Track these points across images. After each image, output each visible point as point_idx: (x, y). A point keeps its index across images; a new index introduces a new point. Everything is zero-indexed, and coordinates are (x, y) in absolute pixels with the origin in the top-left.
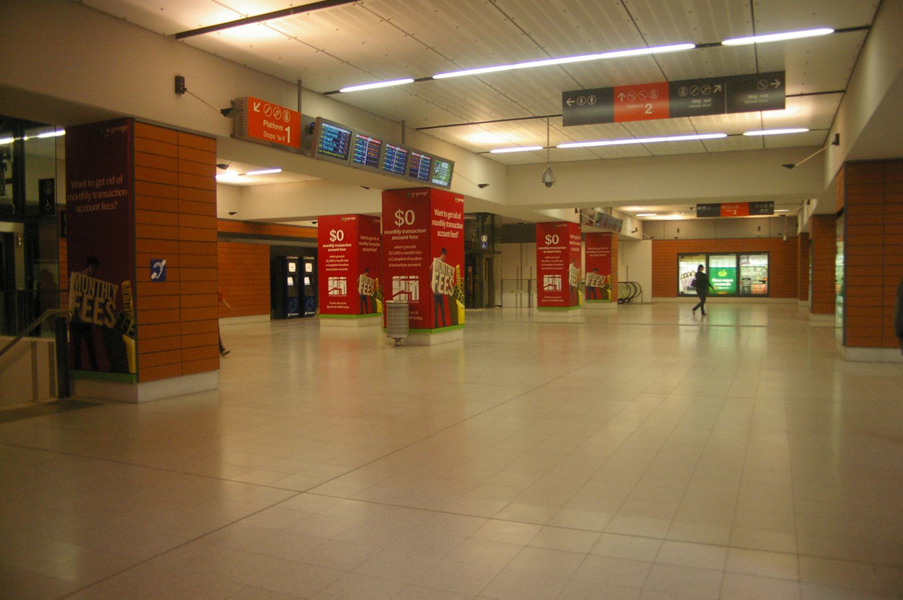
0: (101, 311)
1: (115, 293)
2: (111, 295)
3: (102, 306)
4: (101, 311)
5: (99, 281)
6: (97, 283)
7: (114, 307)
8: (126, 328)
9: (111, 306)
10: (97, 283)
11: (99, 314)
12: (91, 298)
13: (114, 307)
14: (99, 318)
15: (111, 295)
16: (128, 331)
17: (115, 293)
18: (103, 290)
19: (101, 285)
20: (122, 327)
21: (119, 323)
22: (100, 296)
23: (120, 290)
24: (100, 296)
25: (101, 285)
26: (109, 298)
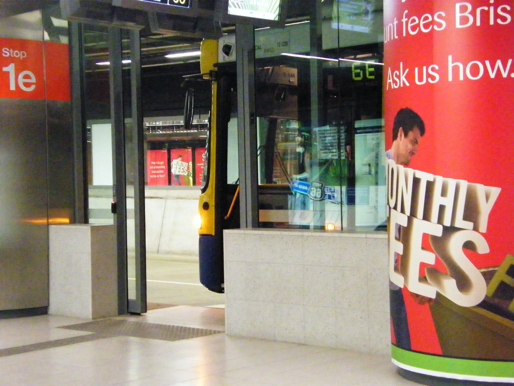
0: (430, 258)
3: (435, 244)
4: (430, 258)
5: (425, 177)
6: (416, 181)
7: (483, 247)
9: (469, 247)
10: (416, 181)
11: (423, 265)
14: (422, 279)
15: (471, 213)
18: (437, 200)
22: (426, 217)
24: (426, 217)
25: (430, 186)
26: (460, 222)
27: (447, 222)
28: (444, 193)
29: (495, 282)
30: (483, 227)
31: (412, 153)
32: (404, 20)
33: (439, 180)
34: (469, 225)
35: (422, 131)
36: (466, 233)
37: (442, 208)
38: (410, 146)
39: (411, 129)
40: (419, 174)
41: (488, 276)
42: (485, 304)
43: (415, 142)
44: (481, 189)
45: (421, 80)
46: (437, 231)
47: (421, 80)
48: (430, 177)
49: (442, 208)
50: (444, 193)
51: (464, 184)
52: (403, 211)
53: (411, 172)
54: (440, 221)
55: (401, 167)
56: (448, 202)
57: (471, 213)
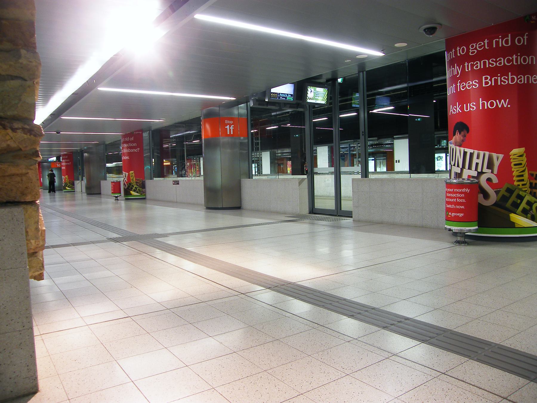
1: (497, 164)
6: (465, 153)
7: (495, 180)
8: (516, 206)
9: (489, 180)
10: (465, 153)
12: (458, 170)
13: (495, 180)
15: (490, 166)
16: (521, 208)
17: (497, 164)
19: (471, 155)
20: (508, 204)
21: (504, 199)
22: (470, 168)
24: (470, 168)
25: (471, 155)
26: (485, 170)
27: (479, 170)
28: (478, 157)
29: (500, 195)
30: (495, 172)
31: (463, 141)
32: (458, 84)
33: (476, 152)
34: (490, 171)
35: (468, 132)
36: (488, 174)
37: (477, 164)
38: (462, 138)
39: (463, 131)
40: (466, 150)
41: (497, 193)
42: (496, 204)
43: (464, 136)
44: (495, 155)
45: (467, 109)
46: (475, 174)
47: (467, 109)
48: (472, 151)
49: (477, 164)
50: (478, 157)
51: (487, 153)
52: (458, 166)
53: (462, 149)
54: (476, 169)
55: (457, 147)
56: (480, 161)
57: (490, 166)
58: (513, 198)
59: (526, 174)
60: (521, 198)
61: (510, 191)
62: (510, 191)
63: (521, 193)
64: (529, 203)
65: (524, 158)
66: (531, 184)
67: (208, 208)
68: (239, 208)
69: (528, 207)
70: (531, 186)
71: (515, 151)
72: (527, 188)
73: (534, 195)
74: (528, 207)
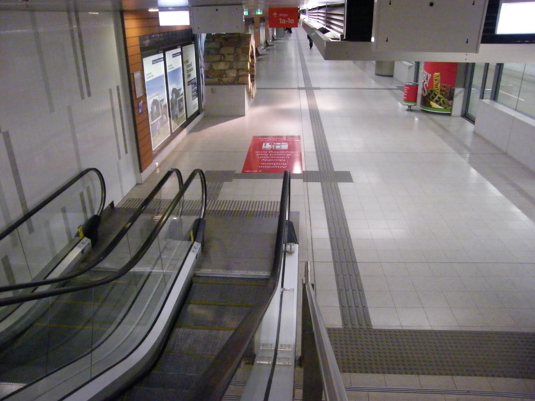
2: (427, 79)
7: (427, 86)
8: (433, 98)
13: (427, 86)
16: (435, 99)
17: (429, 78)
20: (430, 97)
21: (429, 94)
23: (432, 78)
42: (426, 96)
44: (429, 74)
58: (432, 95)
59: (439, 85)
60: (436, 95)
61: (432, 91)
62: (432, 91)
63: (436, 93)
64: (439, 98)
65: (439, 78)
66: (441, 90)
67: (377, 75)
68: (392, 76)
69: (438, 100)
70: (441, 90)
71: (437, 74)
72: (439, 91)
73: (442, 94)
74: (438, 100)
